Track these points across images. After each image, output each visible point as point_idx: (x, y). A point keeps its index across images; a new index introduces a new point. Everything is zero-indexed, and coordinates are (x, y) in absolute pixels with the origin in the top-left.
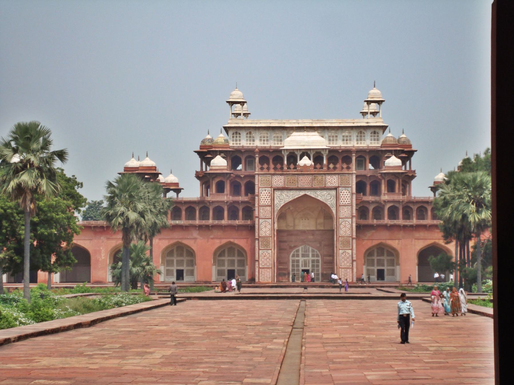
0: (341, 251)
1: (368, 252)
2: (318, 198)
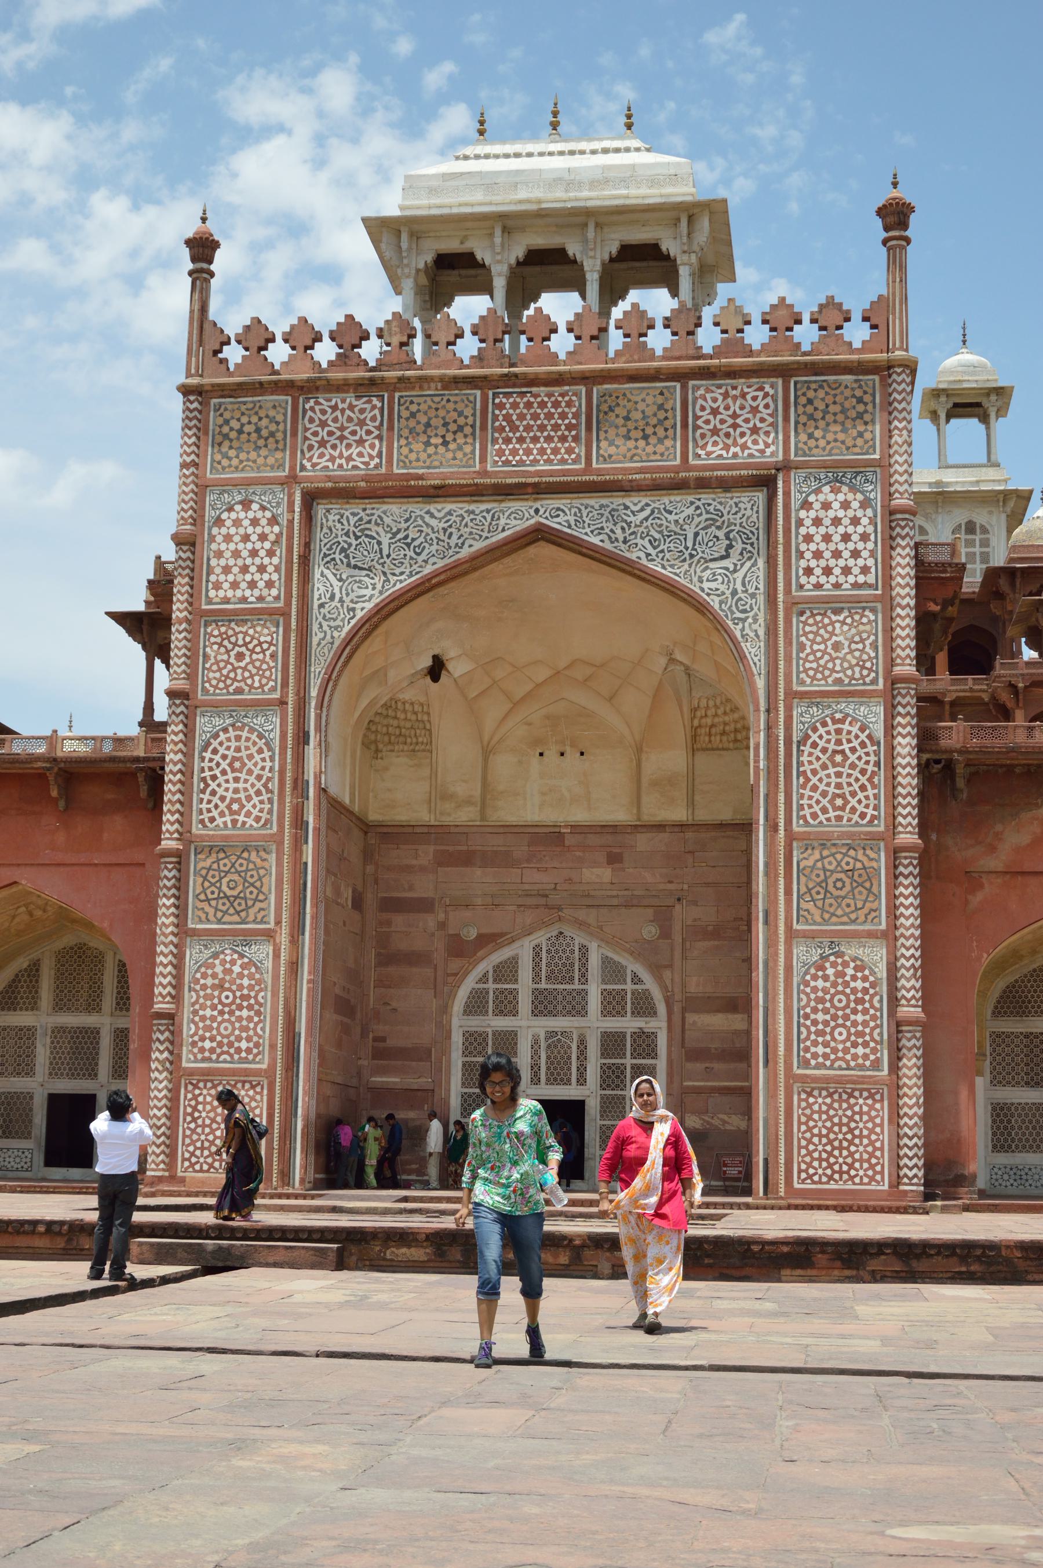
0: (804, 954)
1: (1000, 985)
2: (633, 556)
